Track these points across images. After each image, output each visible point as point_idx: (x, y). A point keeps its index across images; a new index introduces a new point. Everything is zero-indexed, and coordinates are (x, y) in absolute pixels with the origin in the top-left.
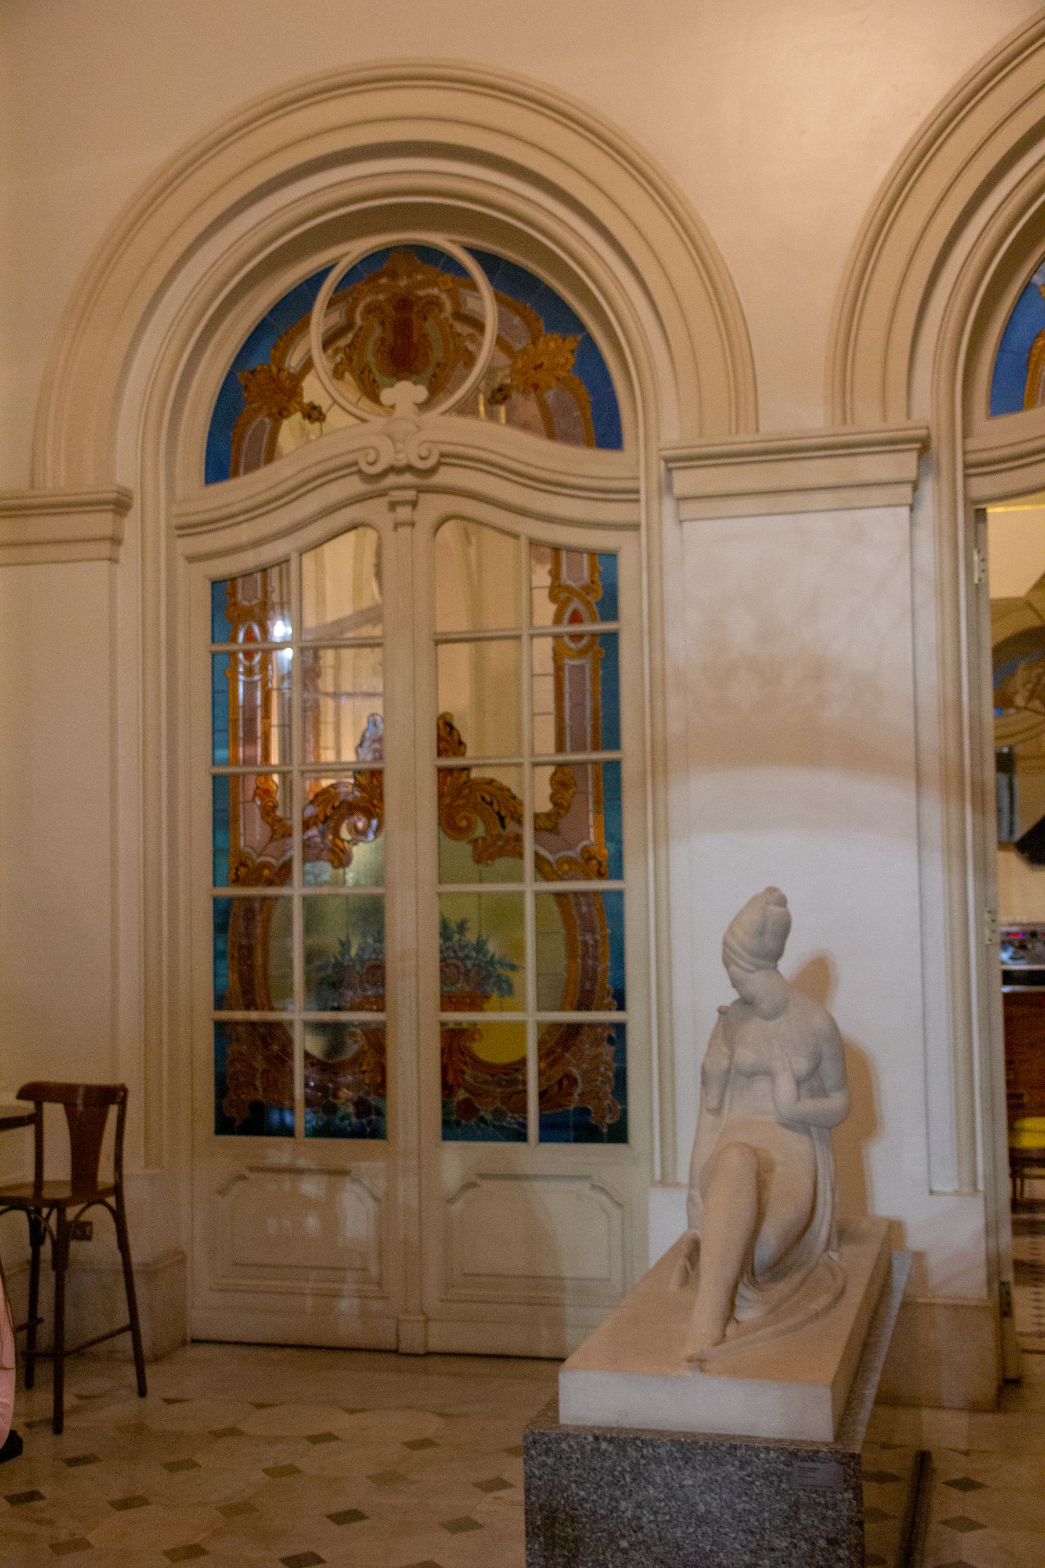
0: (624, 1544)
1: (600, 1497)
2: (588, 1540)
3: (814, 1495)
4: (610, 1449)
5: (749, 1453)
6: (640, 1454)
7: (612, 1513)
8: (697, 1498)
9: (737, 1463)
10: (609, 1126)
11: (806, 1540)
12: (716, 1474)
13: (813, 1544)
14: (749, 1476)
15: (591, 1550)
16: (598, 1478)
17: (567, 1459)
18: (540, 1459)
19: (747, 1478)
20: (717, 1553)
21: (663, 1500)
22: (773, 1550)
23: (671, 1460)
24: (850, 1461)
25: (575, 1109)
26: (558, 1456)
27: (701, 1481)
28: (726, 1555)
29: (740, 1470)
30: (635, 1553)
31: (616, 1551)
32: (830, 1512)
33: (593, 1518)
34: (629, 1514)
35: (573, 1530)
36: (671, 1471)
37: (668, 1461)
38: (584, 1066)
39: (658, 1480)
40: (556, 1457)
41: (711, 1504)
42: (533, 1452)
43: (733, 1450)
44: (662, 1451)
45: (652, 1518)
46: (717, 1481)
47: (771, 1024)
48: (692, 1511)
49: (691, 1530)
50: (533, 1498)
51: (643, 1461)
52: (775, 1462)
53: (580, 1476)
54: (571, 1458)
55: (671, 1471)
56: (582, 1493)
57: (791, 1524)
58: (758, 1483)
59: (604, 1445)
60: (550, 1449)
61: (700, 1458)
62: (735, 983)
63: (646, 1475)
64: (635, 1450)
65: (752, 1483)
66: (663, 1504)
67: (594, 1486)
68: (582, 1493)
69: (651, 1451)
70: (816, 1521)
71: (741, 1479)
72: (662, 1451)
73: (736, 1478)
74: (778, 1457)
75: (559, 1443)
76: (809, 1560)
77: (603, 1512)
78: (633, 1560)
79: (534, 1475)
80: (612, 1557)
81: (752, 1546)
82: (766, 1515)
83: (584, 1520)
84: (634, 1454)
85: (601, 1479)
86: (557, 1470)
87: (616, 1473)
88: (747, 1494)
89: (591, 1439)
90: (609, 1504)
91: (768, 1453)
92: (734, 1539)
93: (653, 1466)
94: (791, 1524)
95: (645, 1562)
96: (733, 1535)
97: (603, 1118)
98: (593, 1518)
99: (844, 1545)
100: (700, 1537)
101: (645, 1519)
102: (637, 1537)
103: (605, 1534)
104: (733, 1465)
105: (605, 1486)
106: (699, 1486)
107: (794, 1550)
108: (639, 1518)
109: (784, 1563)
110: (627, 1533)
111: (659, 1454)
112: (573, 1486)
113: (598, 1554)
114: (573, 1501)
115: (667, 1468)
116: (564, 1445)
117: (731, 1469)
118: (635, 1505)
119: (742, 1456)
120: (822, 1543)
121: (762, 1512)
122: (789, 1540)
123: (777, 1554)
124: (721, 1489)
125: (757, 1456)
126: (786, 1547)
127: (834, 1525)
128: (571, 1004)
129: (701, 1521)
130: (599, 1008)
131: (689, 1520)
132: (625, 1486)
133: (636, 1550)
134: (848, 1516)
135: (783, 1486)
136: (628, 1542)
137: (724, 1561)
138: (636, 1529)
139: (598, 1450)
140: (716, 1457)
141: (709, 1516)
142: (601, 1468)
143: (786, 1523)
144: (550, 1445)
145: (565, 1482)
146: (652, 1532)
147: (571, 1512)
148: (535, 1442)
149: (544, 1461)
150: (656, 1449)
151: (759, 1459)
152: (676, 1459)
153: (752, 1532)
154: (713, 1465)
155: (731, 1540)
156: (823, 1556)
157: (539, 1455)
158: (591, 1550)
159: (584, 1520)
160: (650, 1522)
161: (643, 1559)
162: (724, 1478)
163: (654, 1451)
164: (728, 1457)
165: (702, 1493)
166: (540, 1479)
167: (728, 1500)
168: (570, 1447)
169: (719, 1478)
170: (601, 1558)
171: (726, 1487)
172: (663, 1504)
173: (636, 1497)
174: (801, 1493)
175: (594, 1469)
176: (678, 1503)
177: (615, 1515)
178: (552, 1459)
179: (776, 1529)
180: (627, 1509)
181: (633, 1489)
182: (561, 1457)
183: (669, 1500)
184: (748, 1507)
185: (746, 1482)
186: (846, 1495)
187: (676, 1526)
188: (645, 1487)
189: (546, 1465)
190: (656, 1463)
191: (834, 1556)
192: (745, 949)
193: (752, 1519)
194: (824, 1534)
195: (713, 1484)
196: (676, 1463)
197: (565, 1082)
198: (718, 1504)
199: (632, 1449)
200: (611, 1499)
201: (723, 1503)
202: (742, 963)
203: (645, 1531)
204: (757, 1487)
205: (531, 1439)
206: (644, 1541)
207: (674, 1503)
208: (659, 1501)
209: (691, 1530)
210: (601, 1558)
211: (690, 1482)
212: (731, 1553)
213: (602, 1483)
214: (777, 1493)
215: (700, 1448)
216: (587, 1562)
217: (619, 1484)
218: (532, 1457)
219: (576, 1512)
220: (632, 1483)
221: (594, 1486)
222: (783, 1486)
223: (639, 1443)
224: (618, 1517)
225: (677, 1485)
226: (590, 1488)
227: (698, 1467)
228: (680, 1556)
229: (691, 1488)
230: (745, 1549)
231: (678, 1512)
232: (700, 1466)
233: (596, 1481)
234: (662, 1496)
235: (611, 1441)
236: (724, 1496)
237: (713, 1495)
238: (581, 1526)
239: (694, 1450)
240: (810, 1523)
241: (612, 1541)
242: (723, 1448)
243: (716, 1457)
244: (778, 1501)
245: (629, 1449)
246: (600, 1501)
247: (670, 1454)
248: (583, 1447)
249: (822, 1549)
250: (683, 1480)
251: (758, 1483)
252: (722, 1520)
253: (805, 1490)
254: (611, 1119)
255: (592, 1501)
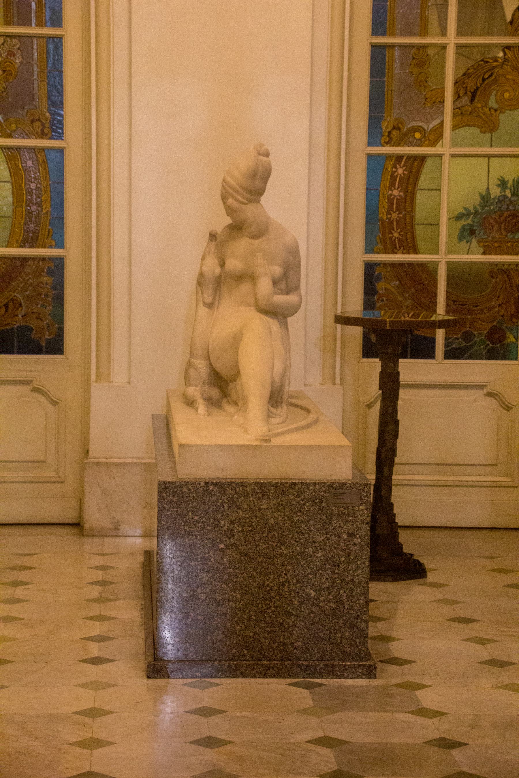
0: (222, 546)
1: (207, 519)
2: (199, 545)
3: (342, 509)
4: (215, 490)
5: (303, 487)
6: (235, 491)
7: (215, 528)
8: (270, 516)
9: (295, 493)
10: (47, 340)
11: (335, 535)
12: (282, 501)
13: (340, 537)
14: (303, 500)
15: (200, 551)
16: (206, 508)
17: (187, 497)
18: (169, 498)
19: (301, 502)
20: (280, 547)
21: (248, 518)
22: (315, 542)
23: (254, 494)
24: (364, 488)
25: (17, 327)
26: (181, 496)
27: (272, 506)
28: (286, 547)
29: (297, 497)
30: (228, 551)
31: (217, 551)
32: (351, 518)
33: (202, 532)
34: (226, 528)
35: (189, 540)
36: (253, 501)
37: (252, 495)
38: (27, 293)
39: (245, 506)
40: (179, 496)
41: (278, 519)
42: (164, 494)
43: (293, 485)
44: (248, 489)
45: (240, 529)
46: (282, 505)
47: (257, 242)
48: (266, 524)
49: (264, 535)
50: (164, 523)
51: (236, 496)
52: (319, 491)
53: (195, 507)
54: (190, 497)
55: (253, 501)
56: (196, 518)
57: (327, 526)
58: (308, 504)
59: (211, 488)
60: (176, 492)
61: (272, 492)
62: (230, 212)
63: (238, 504)
64: (231, 489)
65: (304, 504)
66: (248, 520)
67: (204, 513)
68: (196, 518)
69: (241, 490)
70: (342, 524)
71: (298, 502)
72: (248, 489)
73: (294, 502)
74: (321, 488)
75: (182, 488)
76: (336, 546)
77: (208, 528)
78: (227, 555)
79: (164, 508)
80: (214, 555)
81: (302, 541)
82: (312, 522)
83: (197, 533)
84: (231, 492)
85: (209, 508)
86: (180, 505)
87: (219, 504)
88: (300, 511)
89: (203, 484)
90: (213, 523)
91: (315, 486)
92: (291, 538)
93: (243, 499)
94: (327, 526)
95: (235, 556)
96: (291, 536)
97: (43, 335)
98: (202, 532)
99: (358, 536)
100: (270, 539)
101: (236, 531)
102: (230, 541)
103: (209, 541)
104: (293, 495)
105: (211, 512)
106: (271, 508)
107: (327, 542)
108: (232, 530)
109: (321, 549)
110: (224, 539)
111: (247, 491)
112: (190, 513)
113: (205, 553)
114: (189, 522)
115: (251, 499)
116: (185, 489)
117: (292, 497)
118: (229, 522)
119: (299, 489)
120: (345, 536)
121: (309, 521)
122: (325, 536)
123: (317, 544)
124: (284, 509)
125: (308, 488)
126: (323, 540)
127: (353, 525)
128: (17, 241)
129: (272, 528)
130: (44, 247)
131: (264, 529)
132: (224, 511)
133: (229, 549)
134: (362, 520)
135: (323, 505)
136: (225, 545)
137: (285, 552)
138: (230, 536)
139: (208, 490)
140: (283, 491)
141: (277, 526)
142: (209, 501)
143: (324, 526)
144: (176, 490)
145: (185, 511)
146: (240, 537)
147: (188, 529)
148: (166, 488)
149: (171, 499)
150: (245, 488)
151: (309, 490)
152: (257, 493)
153: (302, 533)
154: (280, 495)
155: (289, 539)
156: (345, 543)
157: (168, 496)
158: (200, 551)
159: (197, 533)
160: (239, 532)
161: (234, 554)
162: (288, 502)
163: (243, 489)
164: (290, 490)
165: (273, 512)
166: (168, 511)
167: (288, 515)
168: (189, 490)
169: (284, 503)
170: (207, 555)
171: (288, 507)
172: (248, 520)
173: (231, 517)
174: (334, 508)
175: (204, 502)
176: (258, 519)
177: (216, 529)
178: (177, 498)
179: (318, 530)
180: (224, 525)
181: (229, 513)
182: (183, 496)
183: (252, 518)
184: (301, 519)
185: (300, 504)
186: (361, 507)
187: (256, 533)
188: (236, 511)
189: (173, 502)
190: (244, 497)
191: (351, 543)
192: (243, 188)
193: (303, 526)
194: (347, 531)
195: (280, 506)
196: (257, 496)
197: (11, 304)
198: (283, 518)
199: (229, 489)
200: (214, 520)
201: (286, 518)
202: (239, 198)
203: (236, 537)
204: (307, 506)
205: (163, 487)
206: (234, 543)
207: (254, 520)
208: (246, 519)
209: (264, 535)
210: (207, 555)
211: (266, 507)
212: (289, 546)
213: (209, 511)
214: (319, 509)
215: (273, 486)
216: (197, 558)
217: (220, 510)
218: (163, 497)
219: (191, 529)
220: (228, 509)
221: (204, 513)
222: (323, 505)
223: (234, 485)
224: (219, 530)
225: (257, 509)
226: (201, 514)
227: (271, 497)
228: (257, 551)
229: (266, 510)
230: (298, 543)
231: (257, 524)
232: (272, 496)
233: (205, 510)
234: (247, 516)
235: (215, 484)
236: (286, 513)
237: (279, 513)
238: (194, 537)
239: (269, 487)
240: (339, 525)
241: (214, 544)
242: (288, 485)
243: (283, 491)
244: (320, 514)
245: (227, 489)
246: (208, 521)
247: (254, 490)
248: (198, 489)
249: (344, 540)
250: (261, 505)
251: (308, 504)
252: (284, 528)
253: (336, 506)
254: (48, 335)
255: (202, 522)
